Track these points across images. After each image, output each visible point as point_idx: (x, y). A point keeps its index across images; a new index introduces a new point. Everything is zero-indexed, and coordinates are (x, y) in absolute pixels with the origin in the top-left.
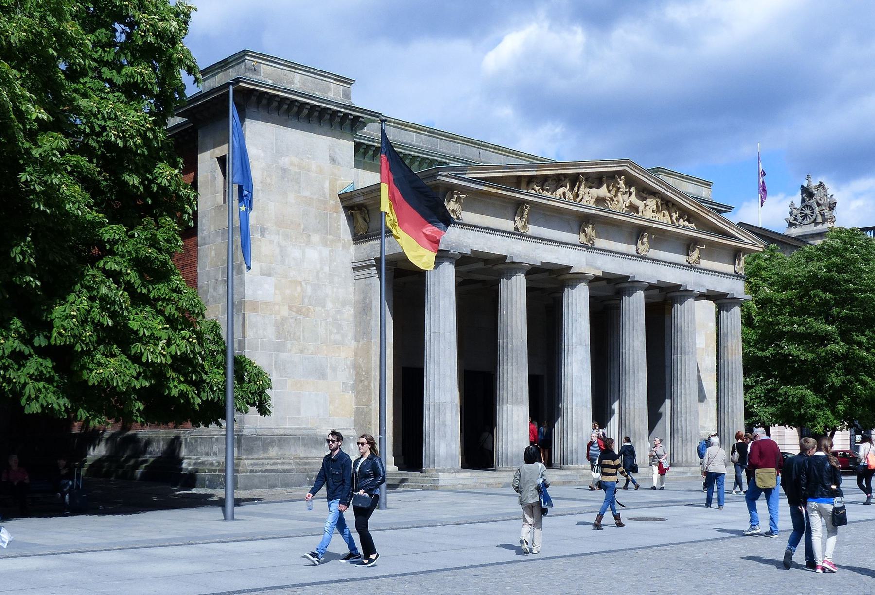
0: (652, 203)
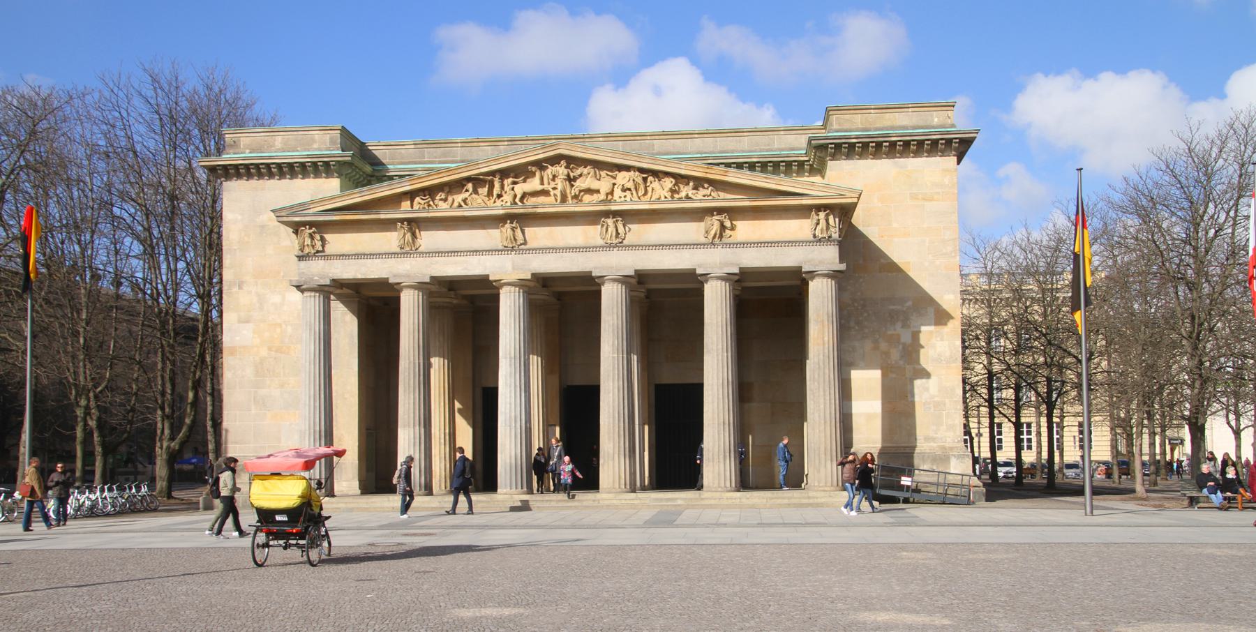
0: (623, 178)
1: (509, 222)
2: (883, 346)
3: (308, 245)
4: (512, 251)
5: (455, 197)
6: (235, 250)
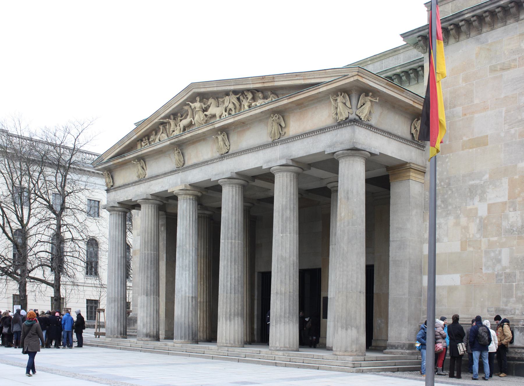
1: (175, 149)
2: (463, 220)
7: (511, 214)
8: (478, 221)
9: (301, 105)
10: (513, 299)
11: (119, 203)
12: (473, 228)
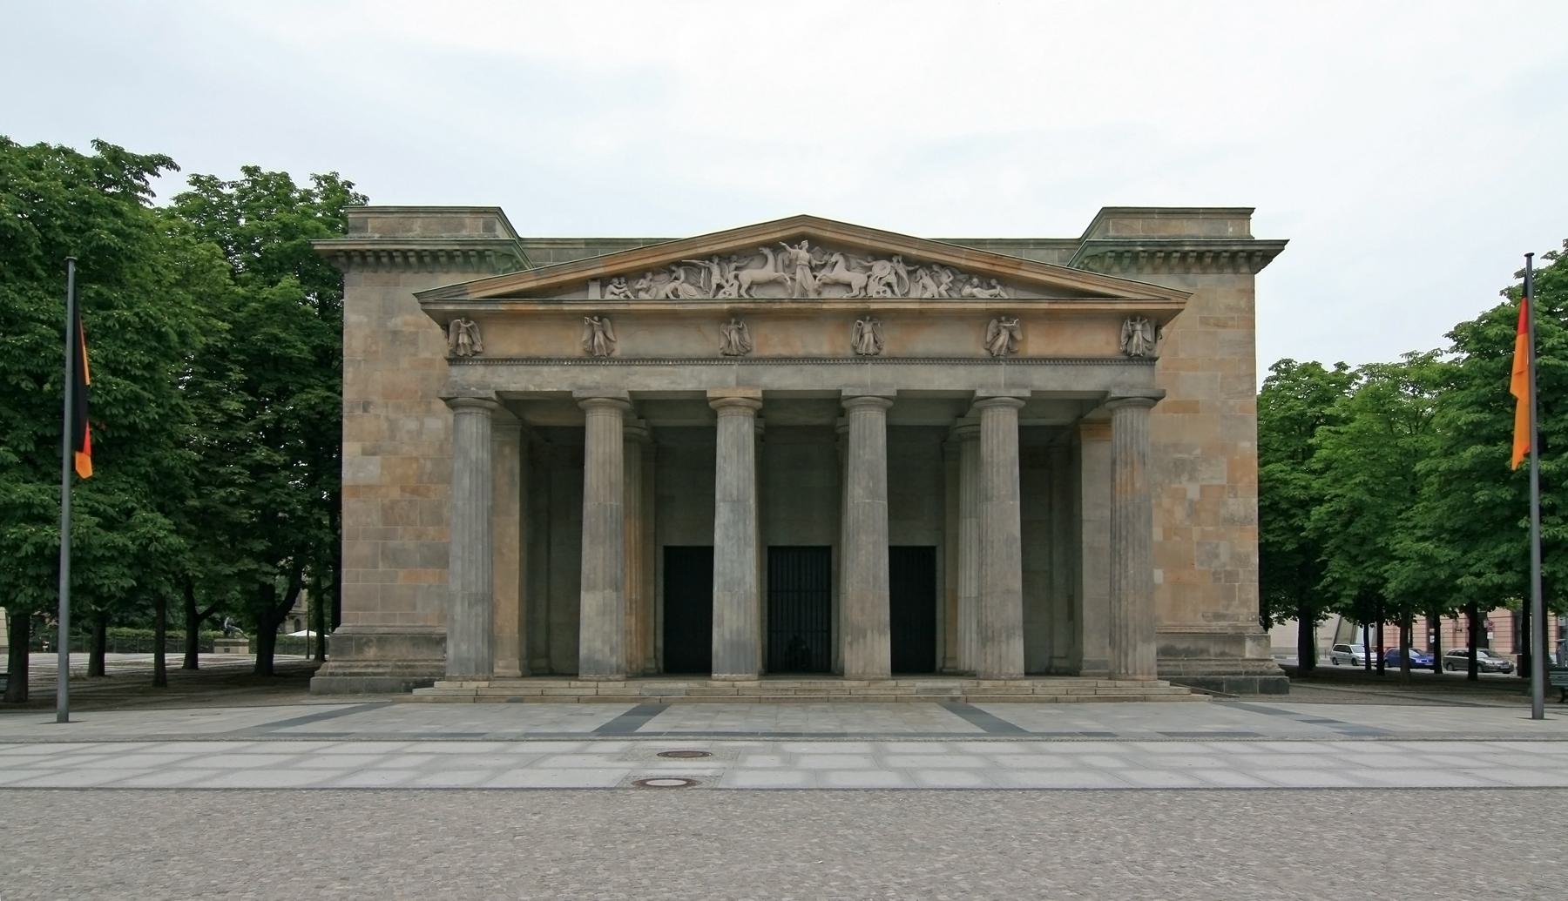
1: (733, 321)
3: (464, 344)
4: (736, 360)
5: (660, 287)
6: (359, 361)
7: (1231, 501)
8: (1187, 505)
9: (1052, 317)
10: (1236, 602)
11: (497, 393)
12: (1180, 513)
